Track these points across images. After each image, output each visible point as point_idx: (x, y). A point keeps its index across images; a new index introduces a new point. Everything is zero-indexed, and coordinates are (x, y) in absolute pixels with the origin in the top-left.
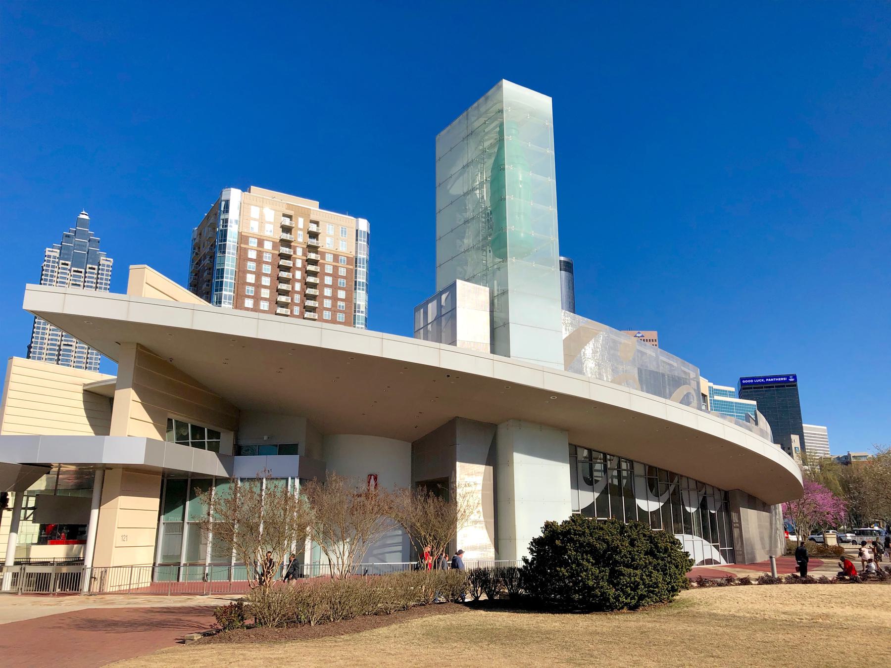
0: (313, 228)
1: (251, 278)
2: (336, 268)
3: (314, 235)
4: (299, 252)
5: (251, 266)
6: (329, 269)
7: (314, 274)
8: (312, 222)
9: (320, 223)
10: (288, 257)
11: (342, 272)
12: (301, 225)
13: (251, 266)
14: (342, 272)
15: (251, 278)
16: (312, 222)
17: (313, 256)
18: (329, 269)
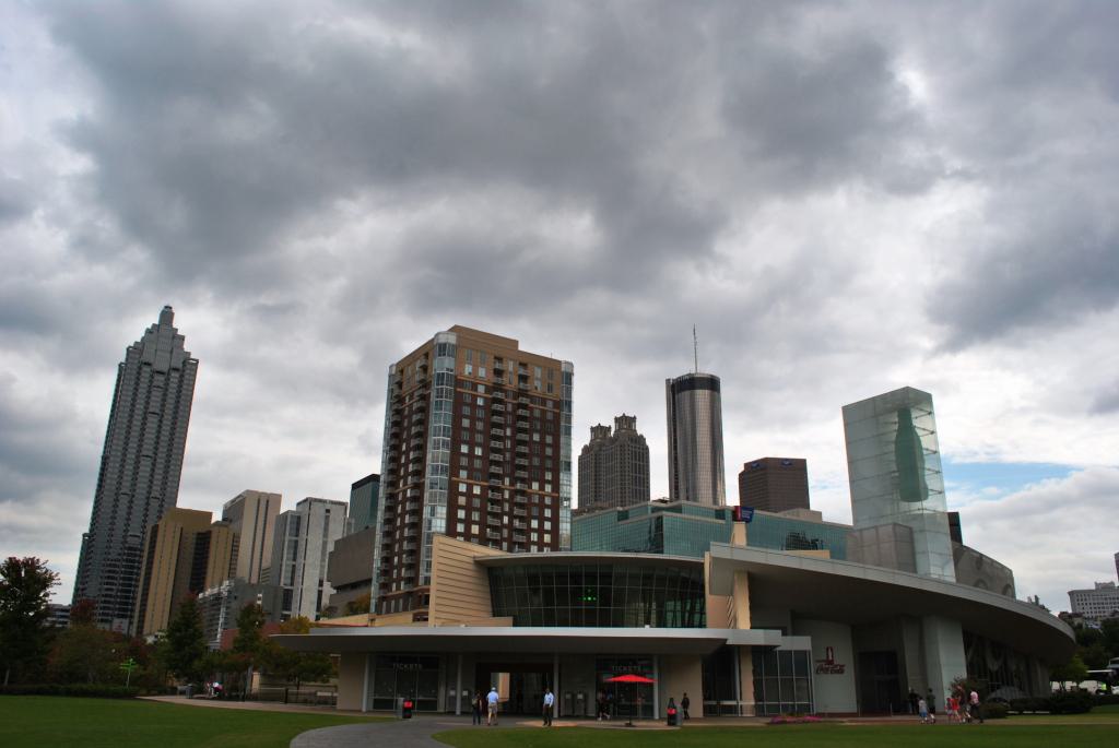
0: (522, 372)
1: (466, 423)
2: (544, 412)
3: (523, 378)
4: (511, 394)
5: (466, 410)
6: (537, 413)
7: (524, 418)
8: (521, 364)
9: (529, 366)
10: (500, 401)
11: (550, 416)
12: (511, 368)
13: (466, 410)
14: (550, 416)
15: (466, 423)
16: (521, 364)
17: (524, 400)
18: (537, 413)
